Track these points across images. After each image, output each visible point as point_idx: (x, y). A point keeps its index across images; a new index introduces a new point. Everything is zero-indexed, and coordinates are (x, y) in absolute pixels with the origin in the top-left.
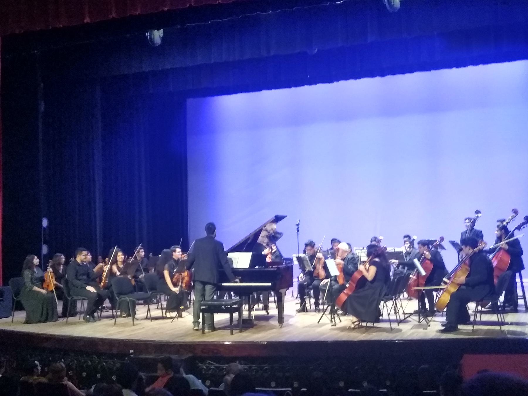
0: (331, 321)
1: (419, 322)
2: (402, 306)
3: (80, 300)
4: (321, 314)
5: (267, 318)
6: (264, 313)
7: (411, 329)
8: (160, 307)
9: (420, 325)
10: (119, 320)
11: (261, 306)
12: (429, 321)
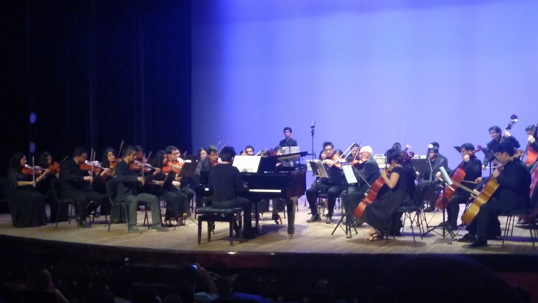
0: (347, 233)
1: (444, 236)
2: (425, 220)
3: (70, 203)
5: (276, 228)
6: (273, 222)
7: (435, 243)
9: (444, 239)
10: (114, 226)
12: (455, 235)
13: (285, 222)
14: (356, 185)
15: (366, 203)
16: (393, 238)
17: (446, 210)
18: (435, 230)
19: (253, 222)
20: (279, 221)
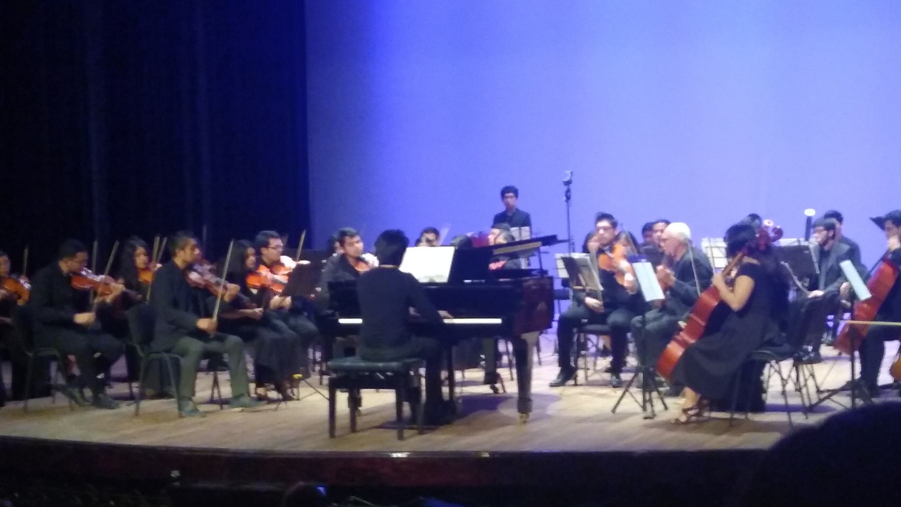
0: (644, 408)
3: (54, 358)
4: (619, 392)
6: (486, 389)
10: (147, 405)
11: (478, 374)
13: (511, 388)
14: (663, 302)
15: (683, 343)
16: (742, 417)
17: (857, 354)
18: (835, 398)
19: (445, 390)
20: (498, 385)
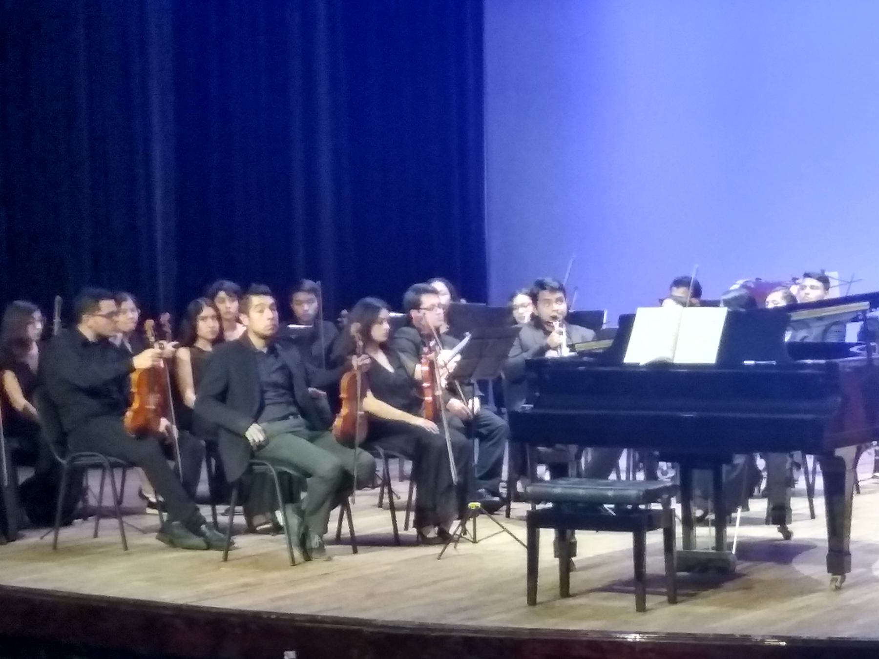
5: (782, 553)
6: (772, 532)
8: (386, 500)
